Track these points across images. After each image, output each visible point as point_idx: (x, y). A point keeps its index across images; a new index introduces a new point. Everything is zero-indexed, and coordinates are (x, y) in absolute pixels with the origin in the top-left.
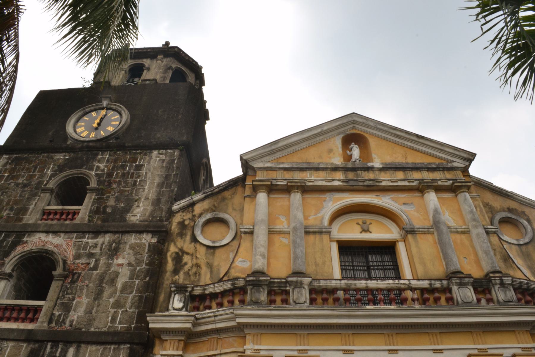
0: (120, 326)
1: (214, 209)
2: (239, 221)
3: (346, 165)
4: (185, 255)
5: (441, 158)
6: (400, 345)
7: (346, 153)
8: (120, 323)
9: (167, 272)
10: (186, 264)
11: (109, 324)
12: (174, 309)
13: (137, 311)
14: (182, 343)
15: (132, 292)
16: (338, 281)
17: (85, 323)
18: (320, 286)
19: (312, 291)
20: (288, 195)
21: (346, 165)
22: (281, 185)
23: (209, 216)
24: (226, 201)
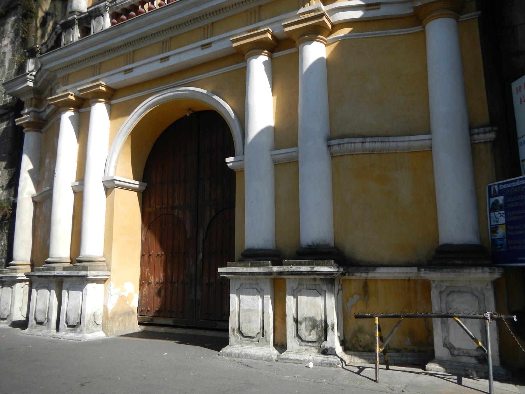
6: (173, 50)
11: (3, 100)
14: (34, 100)
15: (14, 66)
18: (117, 8)
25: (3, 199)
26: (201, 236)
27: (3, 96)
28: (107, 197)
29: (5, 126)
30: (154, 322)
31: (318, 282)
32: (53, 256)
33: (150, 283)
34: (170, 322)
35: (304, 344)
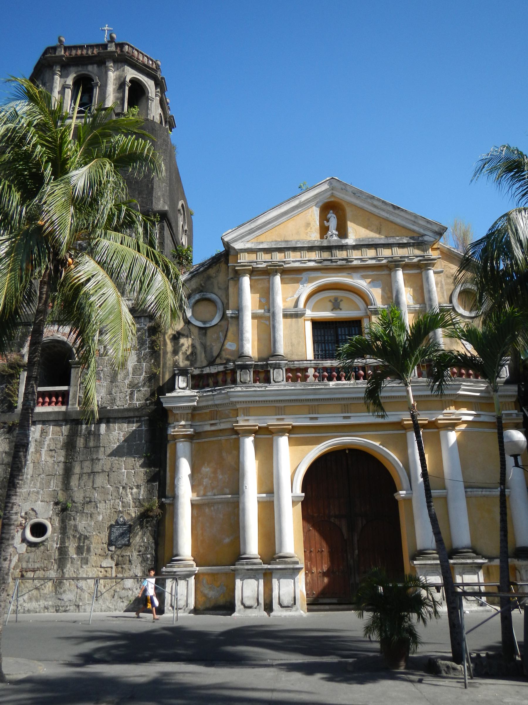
0: (138, 403)
1: (201, 288)
2: (225, 301)
3: (322, 242)
4: (181, 337)
5: (414, 231)
7: (324, 223)
8: (137, 400)
9: (167, 353)
10: (183, 345)
12: (180, 388)
13: (149, 389)
14: (190, 415)
15: (142, 373)
16: (309, 362)
17: (108, 402)
18: (294, 366)
19: (288, 370)
20: (267, 277)
21: (322, 242)
22: (262, 267)
23: (197, 297)
24: (212, 279)
25: (141, 497)
26: (356, 539)
27: (128, 397)
28: (293, 507)
29: (134, 428)
30: (319, 602)
31: (474, 568)
32: (251, 553)
33: (313, 573)
34: (335, 601)
35: (469, 602)
